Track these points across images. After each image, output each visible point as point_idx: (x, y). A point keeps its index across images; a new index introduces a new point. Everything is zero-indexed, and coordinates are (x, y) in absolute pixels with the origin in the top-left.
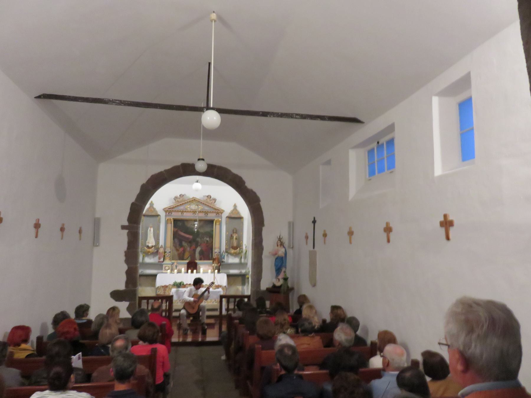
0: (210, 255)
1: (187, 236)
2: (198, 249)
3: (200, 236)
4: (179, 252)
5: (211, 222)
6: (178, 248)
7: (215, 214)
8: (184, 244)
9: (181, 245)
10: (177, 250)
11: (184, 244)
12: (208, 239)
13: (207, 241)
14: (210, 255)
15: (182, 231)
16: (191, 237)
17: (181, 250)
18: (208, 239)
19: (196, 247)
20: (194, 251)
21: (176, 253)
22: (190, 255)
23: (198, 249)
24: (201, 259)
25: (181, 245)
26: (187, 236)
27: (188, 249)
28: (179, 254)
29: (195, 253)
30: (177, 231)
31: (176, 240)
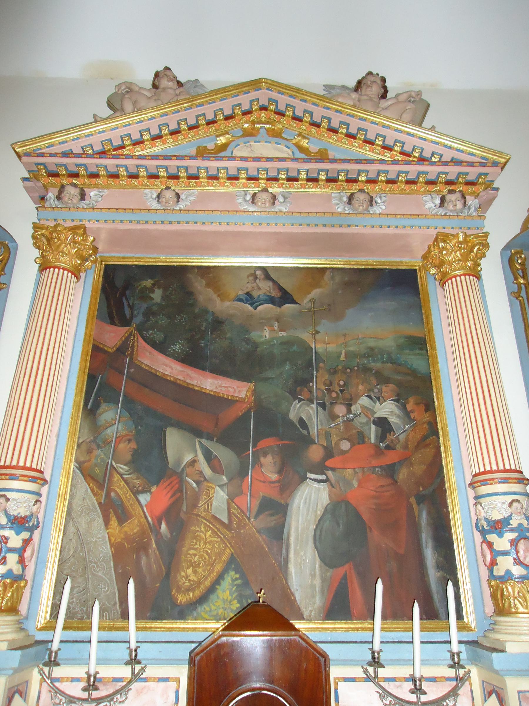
0: (430, 556)
1: (209, 383)
2: (310, 501)
3: (318, 384)
4: (132, 527)
5: (403, 284)
6: (120, 489)
7: (431, 203)
8: (179, 447)
9: (150, 463)
10: (113, 509)
11: (179, 447)
12: (387, 409)
13: (383, 424)
14: (430, 556)
15: (161, 347)
16: (238, 390)
17: (147, 502)
18: (387, 409)
19: (289, 484)
20: (276, 509)
21: (101, 538)
22: (232, 563)
23: (310, 501)
24: (339, 607)
25: (150, 463)
26: (209, 383)
27: (219, 499)
28: (126, 557)
29: (278, 534)
30: (124, 349)
31: (113, 419)
